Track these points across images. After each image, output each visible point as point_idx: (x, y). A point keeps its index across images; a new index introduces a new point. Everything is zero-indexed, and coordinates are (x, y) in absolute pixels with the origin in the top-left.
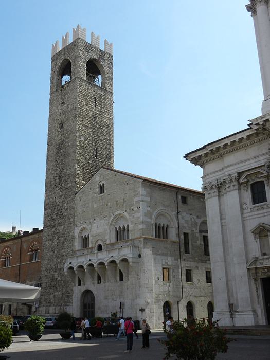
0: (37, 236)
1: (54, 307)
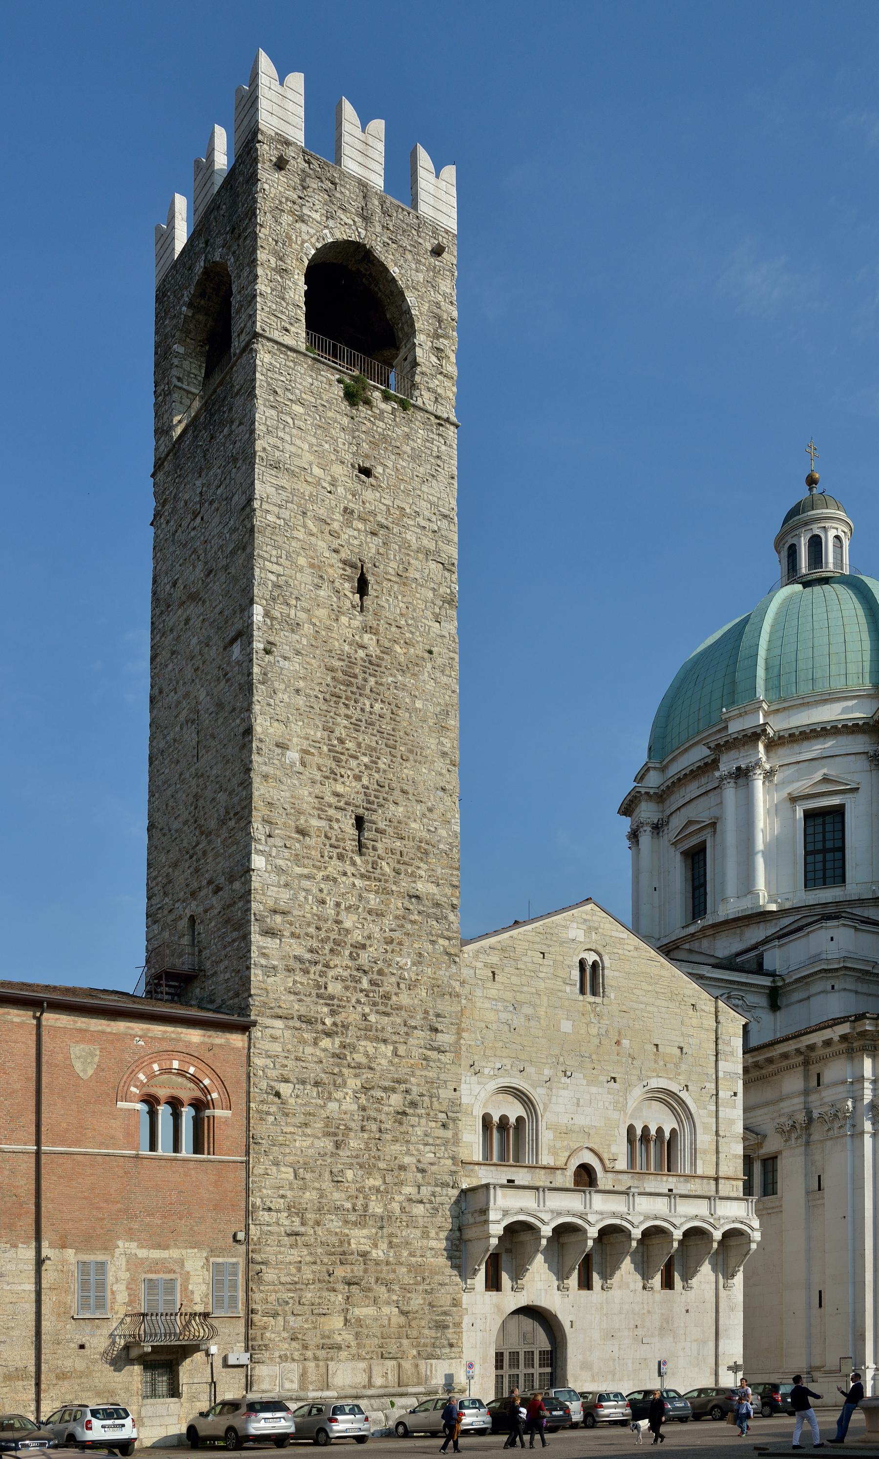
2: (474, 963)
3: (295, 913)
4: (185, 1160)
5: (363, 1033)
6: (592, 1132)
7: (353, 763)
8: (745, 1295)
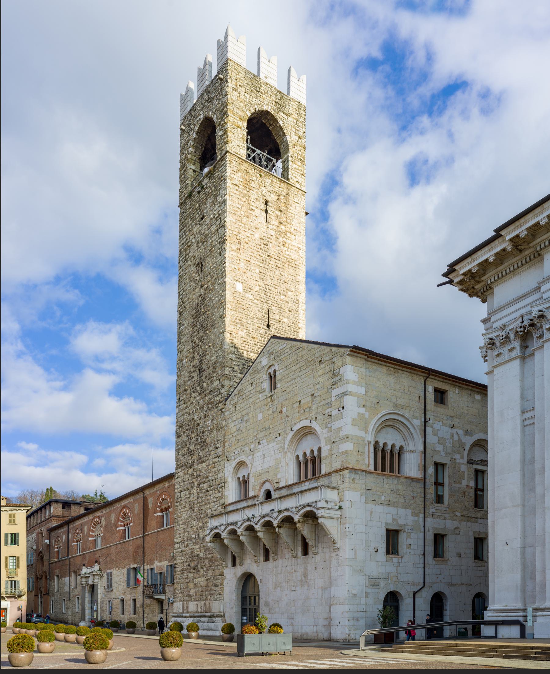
0: (167, 485)
1: (196, 603)
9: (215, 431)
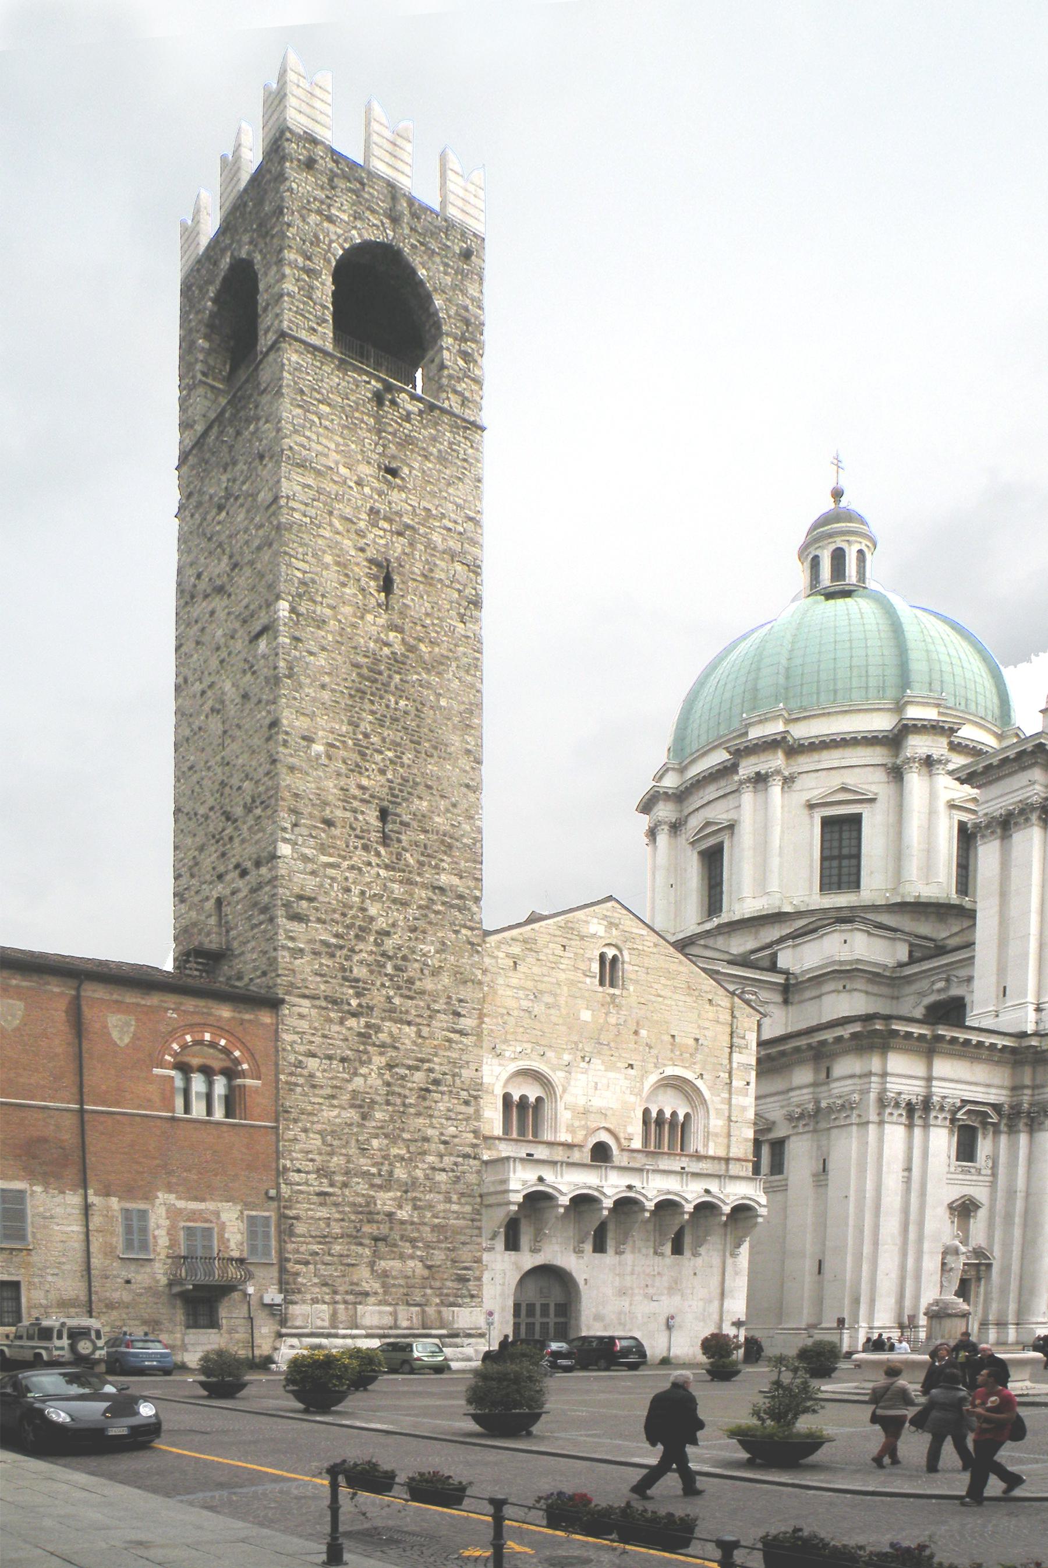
2: (496, 953)
3: (321, 899)
4: (218, 1124)
5: (387, 1014)
6: (609, 1113)
7: (378, 757)
8: (750, 1262)
9: (446, 979)
